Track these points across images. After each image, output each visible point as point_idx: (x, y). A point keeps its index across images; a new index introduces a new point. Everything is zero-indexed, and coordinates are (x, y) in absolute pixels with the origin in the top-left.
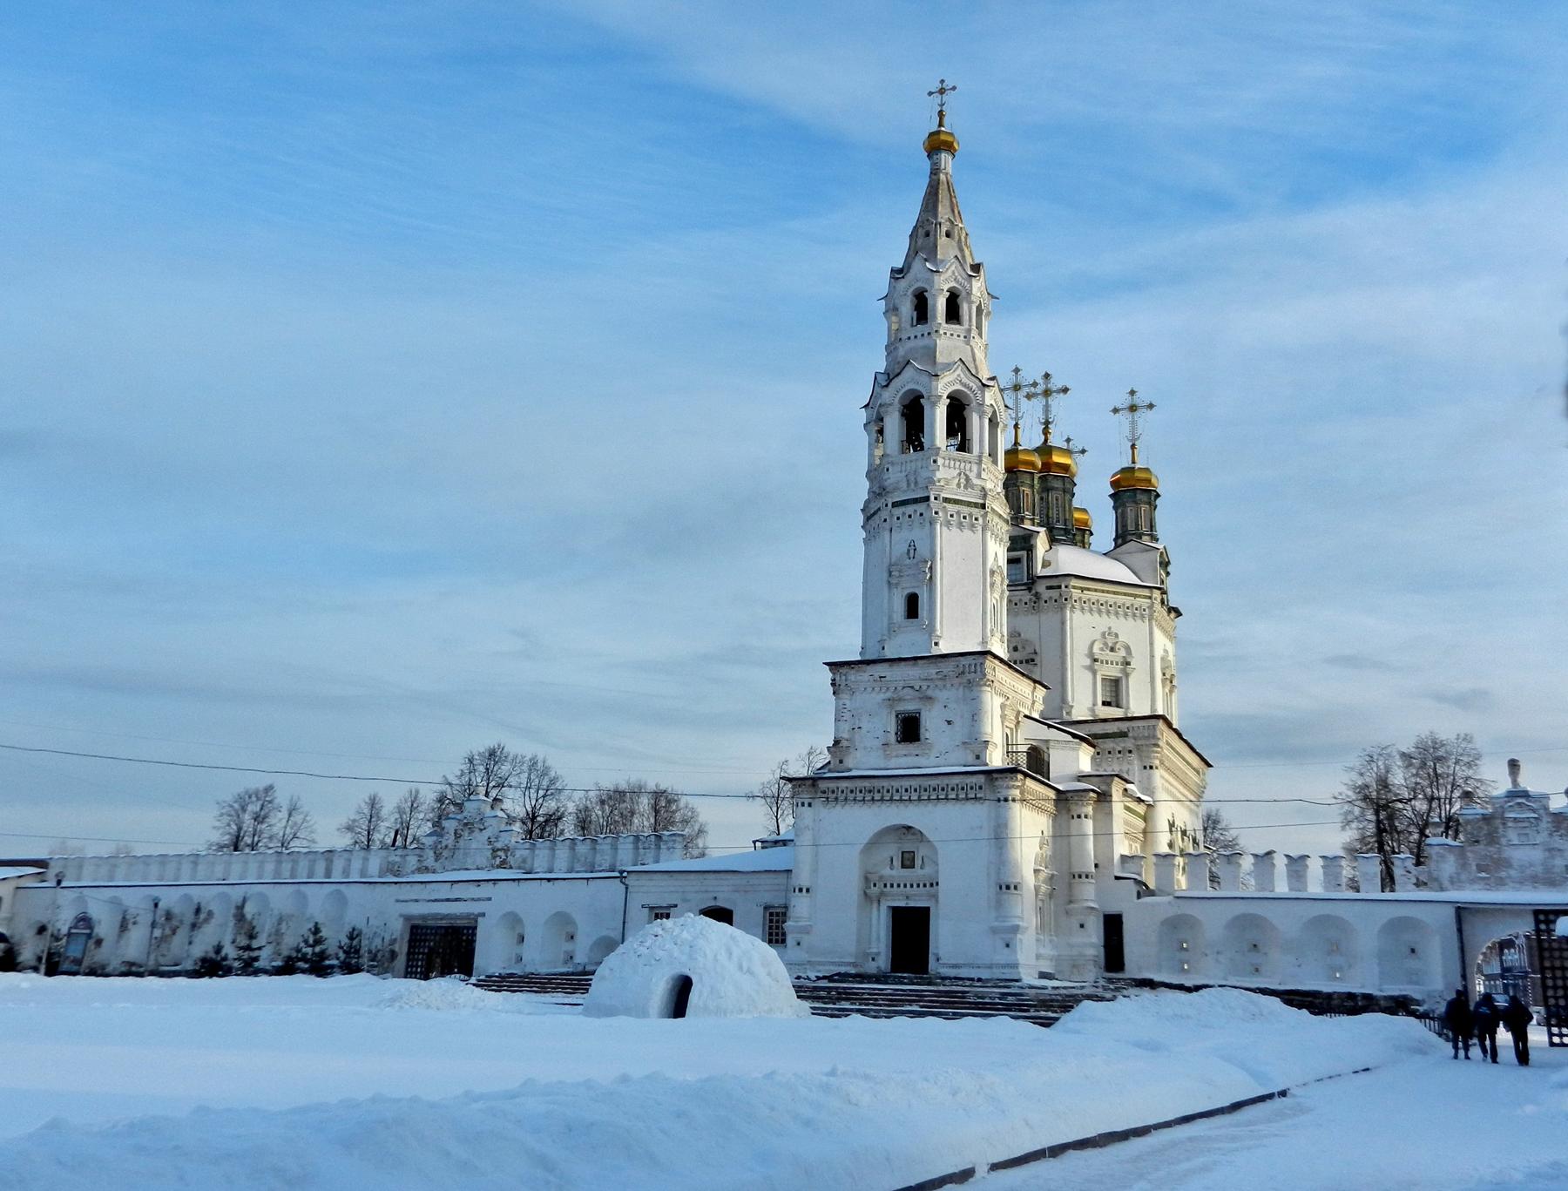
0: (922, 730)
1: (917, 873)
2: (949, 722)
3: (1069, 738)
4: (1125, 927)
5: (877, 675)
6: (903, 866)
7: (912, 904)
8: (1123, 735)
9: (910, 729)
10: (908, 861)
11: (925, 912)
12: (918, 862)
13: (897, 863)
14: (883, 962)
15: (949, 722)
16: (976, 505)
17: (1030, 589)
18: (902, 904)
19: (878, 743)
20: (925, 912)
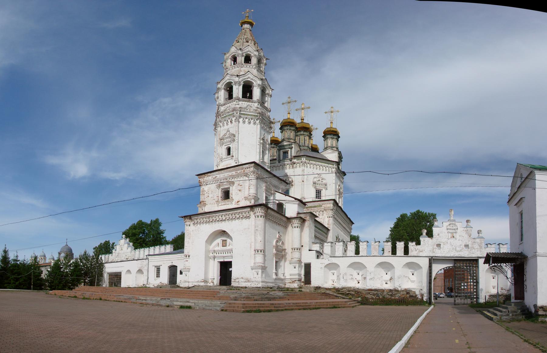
0: (230, 195)
1: (228, 248)
2: (240, 190)
3: (294, 200)
4: (312, 268)
5: (214, 177)
6: (223, 246)
7: (226, 260)
8: (320, 206)
9: (226, 195)
10: (224, 244)
11: (231, 262)
12: (228, 244)
13: (221, 245)
14: (217, 281)
15: (240, 190)
16: (254, 116)
17: (291, 161)
18: (222, 260)
19: (214, 201)
20: (231, 262)
